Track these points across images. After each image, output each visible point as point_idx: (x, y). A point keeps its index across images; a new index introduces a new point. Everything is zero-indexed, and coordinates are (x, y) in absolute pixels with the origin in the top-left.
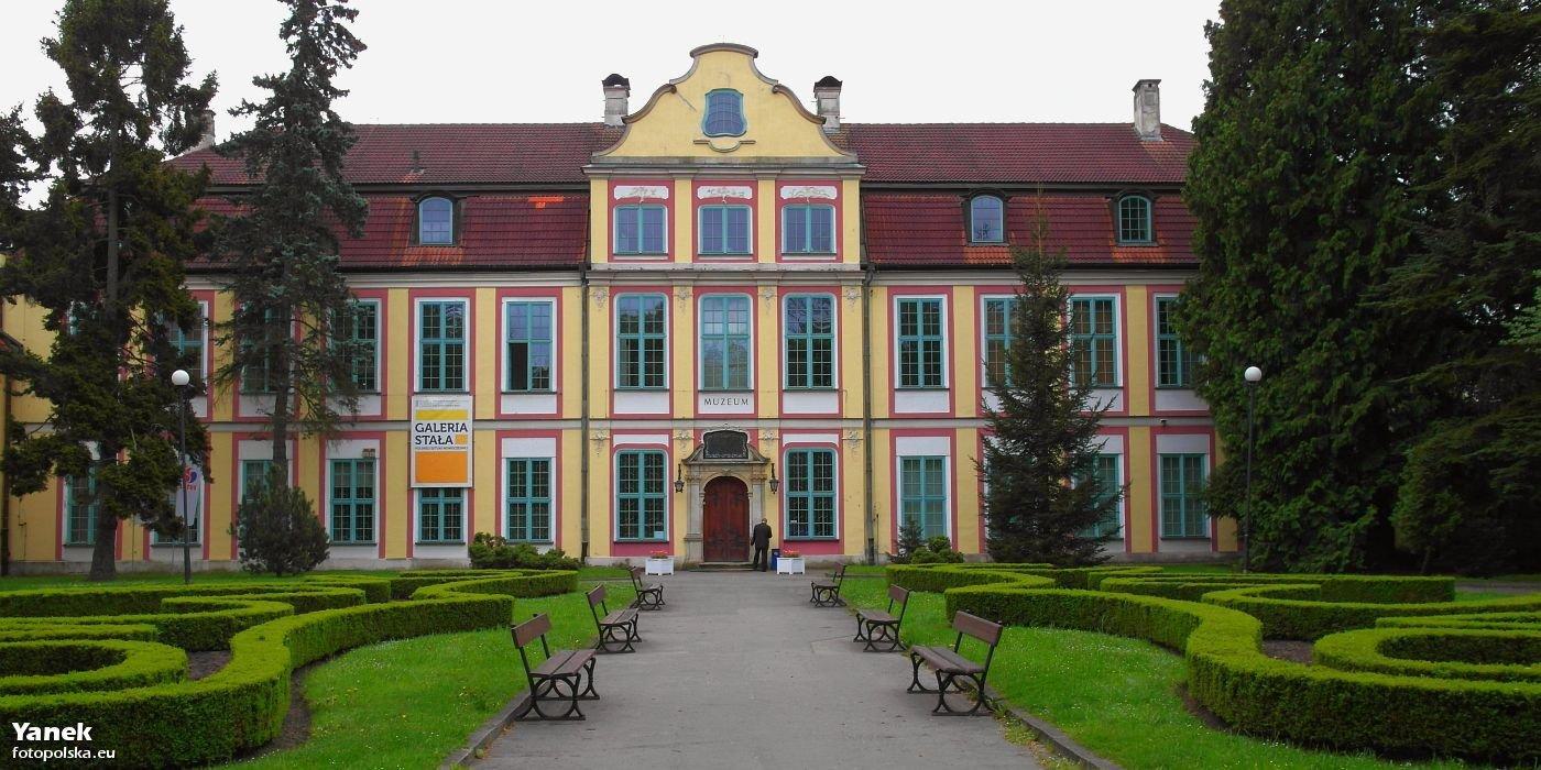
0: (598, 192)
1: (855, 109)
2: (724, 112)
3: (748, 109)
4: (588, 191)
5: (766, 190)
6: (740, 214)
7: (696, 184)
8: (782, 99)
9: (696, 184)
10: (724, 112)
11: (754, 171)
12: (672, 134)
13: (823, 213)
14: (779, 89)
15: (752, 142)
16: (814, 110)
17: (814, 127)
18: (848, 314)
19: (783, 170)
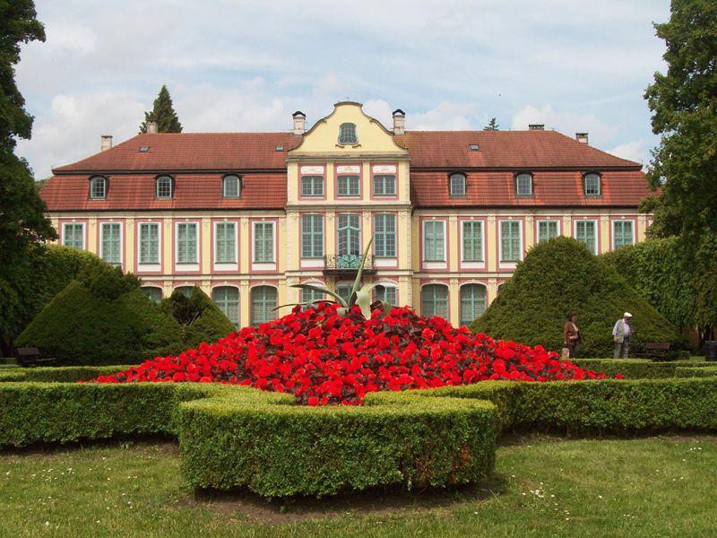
0: (293, 172)
1: (418, 123)
2: (348, 134)
3: (358, 132)
4: (284, 171)
5: (366, 167)
6: (355, 178)
7: (336, 165)
8: (375, 126)
9: (336, 165)
10: (348, 134)
11: (359, 160)
12: (323, 141)
13: (391, 178)
14: (373, 120)
15: (360, 145)
16: (390, 127)
17: (389, 138)
18: (404, 222)
19: (375, 160)
